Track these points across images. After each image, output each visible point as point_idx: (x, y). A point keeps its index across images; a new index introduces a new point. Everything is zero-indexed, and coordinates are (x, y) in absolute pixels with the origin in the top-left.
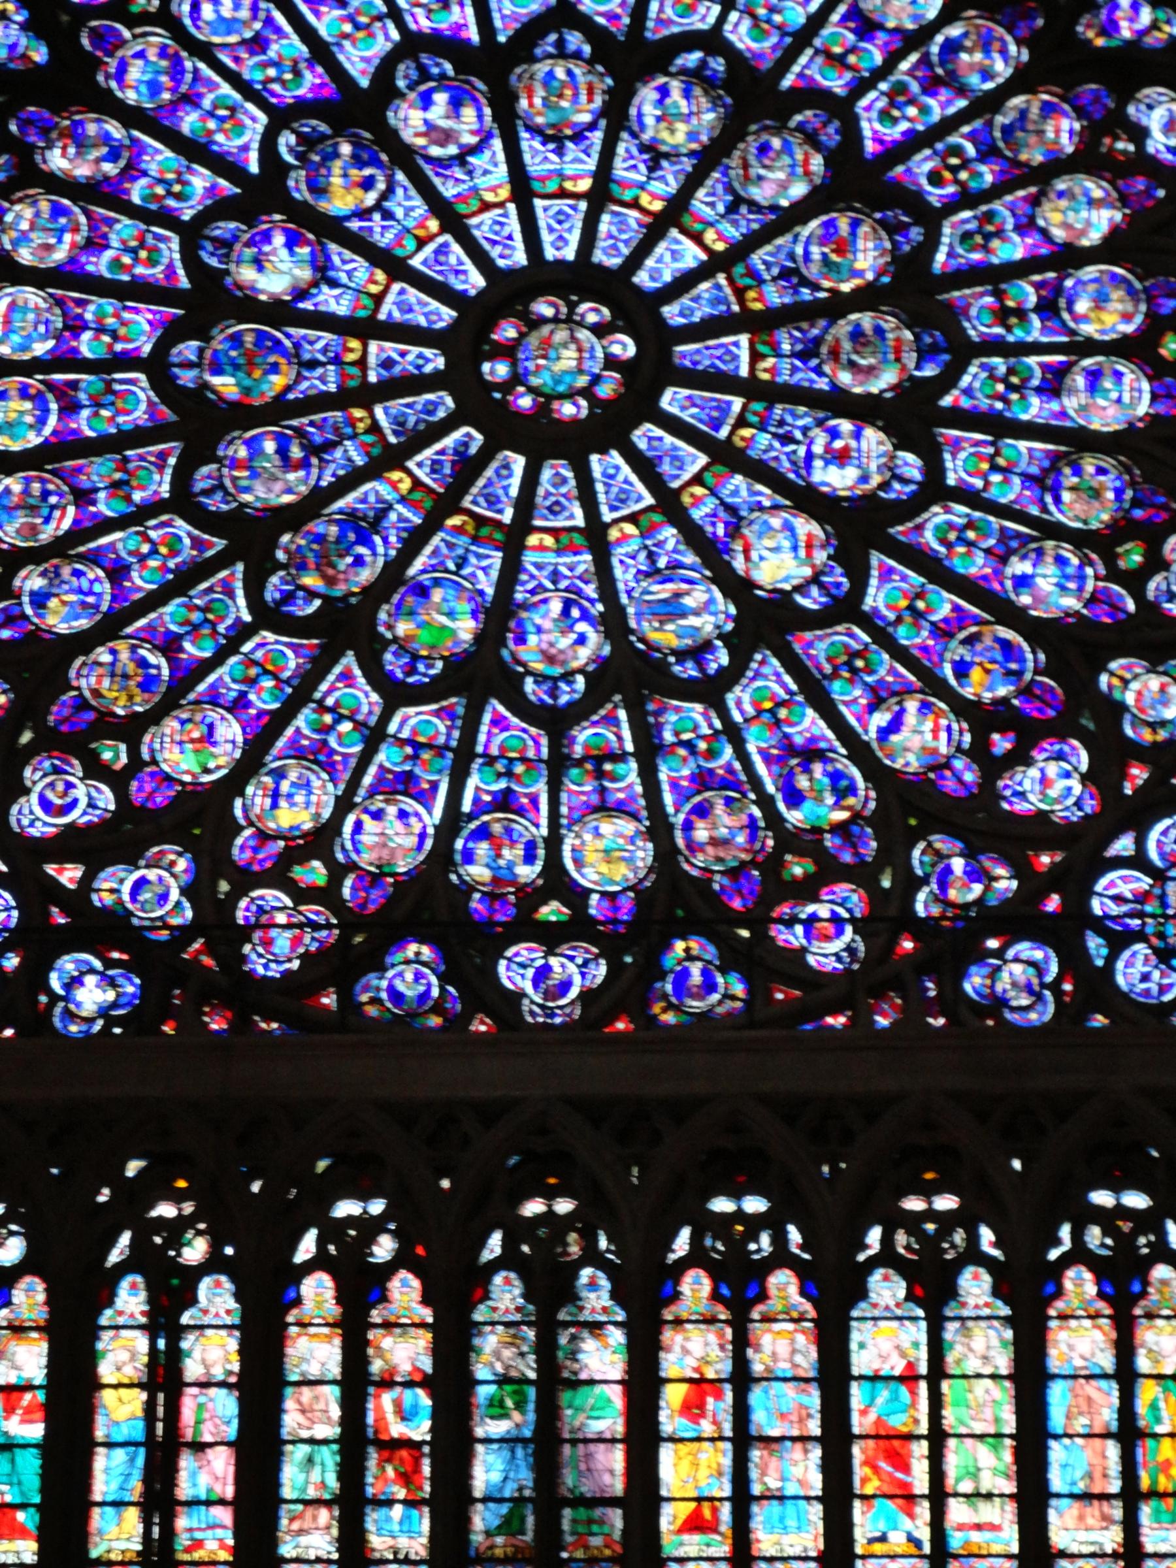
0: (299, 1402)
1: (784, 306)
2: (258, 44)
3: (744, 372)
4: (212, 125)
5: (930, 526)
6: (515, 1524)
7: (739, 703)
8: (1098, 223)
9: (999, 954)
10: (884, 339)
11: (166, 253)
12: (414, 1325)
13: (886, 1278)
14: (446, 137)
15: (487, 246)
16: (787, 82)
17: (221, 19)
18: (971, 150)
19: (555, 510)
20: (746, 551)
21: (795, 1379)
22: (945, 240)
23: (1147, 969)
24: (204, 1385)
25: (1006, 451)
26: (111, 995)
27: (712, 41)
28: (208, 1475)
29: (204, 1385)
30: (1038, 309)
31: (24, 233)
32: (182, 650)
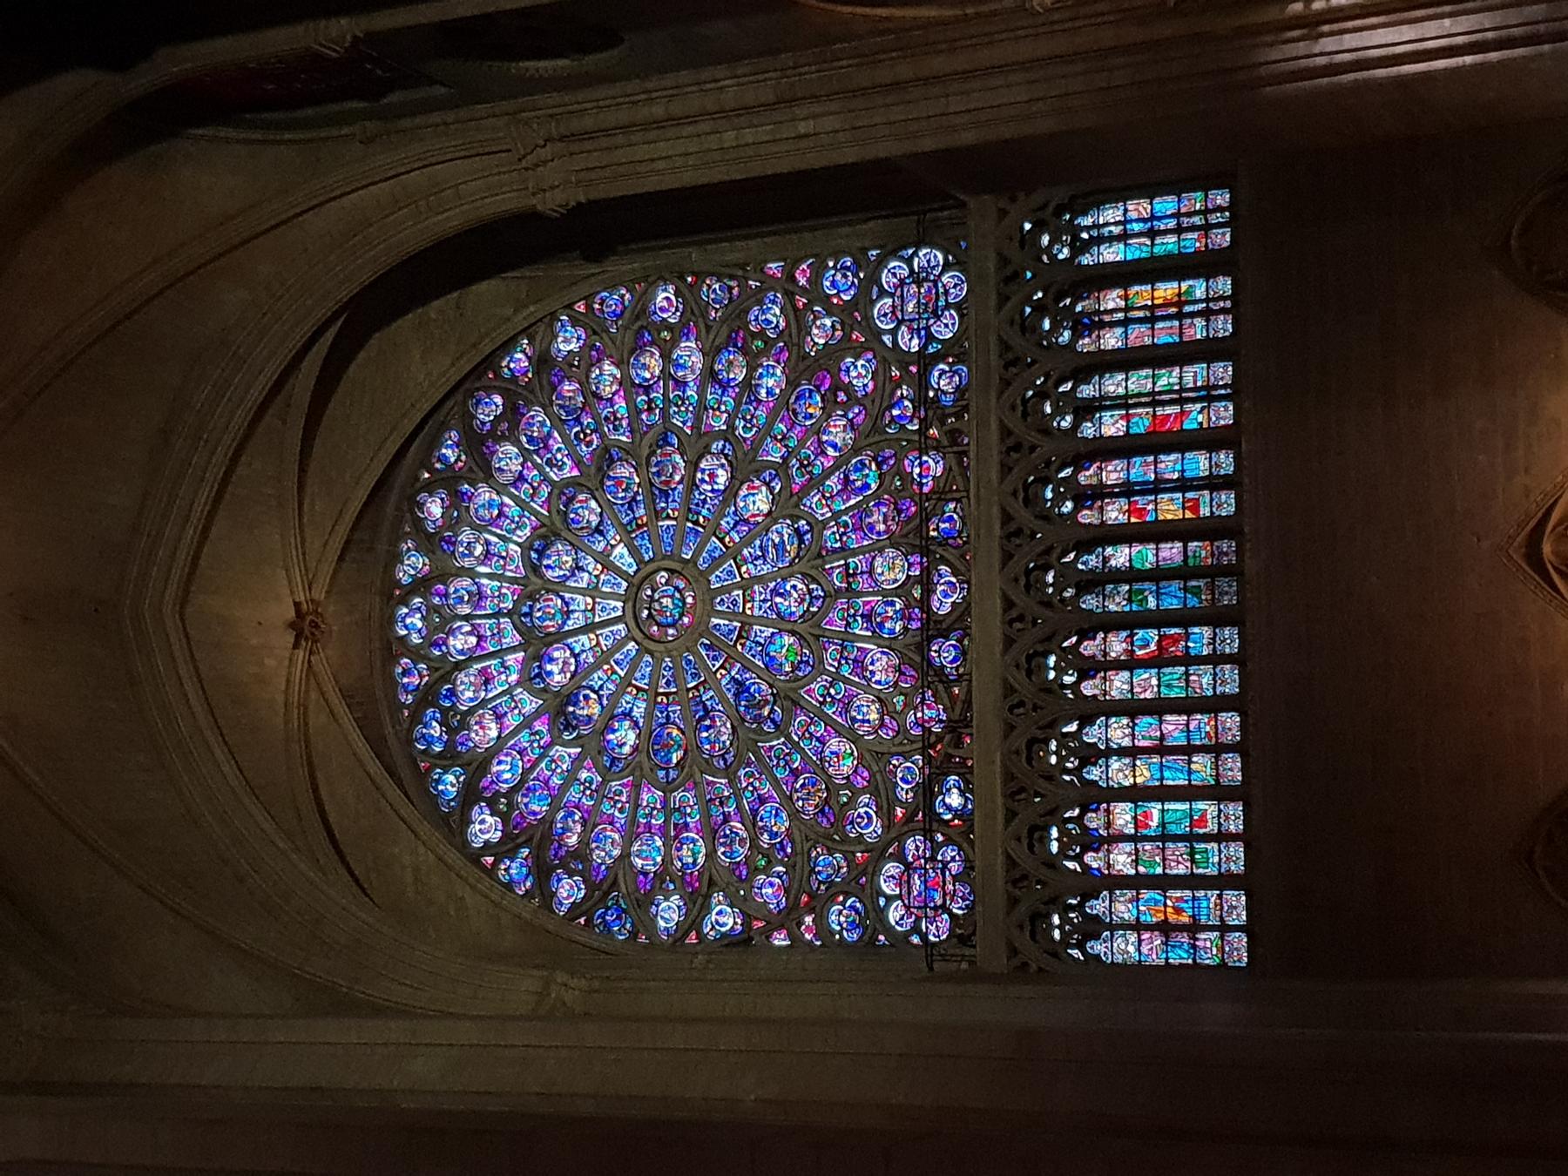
9: (936, 391)
14: (565, 663)
20: (754, 516)
28: (1173, 726)
29: (1133, 735)
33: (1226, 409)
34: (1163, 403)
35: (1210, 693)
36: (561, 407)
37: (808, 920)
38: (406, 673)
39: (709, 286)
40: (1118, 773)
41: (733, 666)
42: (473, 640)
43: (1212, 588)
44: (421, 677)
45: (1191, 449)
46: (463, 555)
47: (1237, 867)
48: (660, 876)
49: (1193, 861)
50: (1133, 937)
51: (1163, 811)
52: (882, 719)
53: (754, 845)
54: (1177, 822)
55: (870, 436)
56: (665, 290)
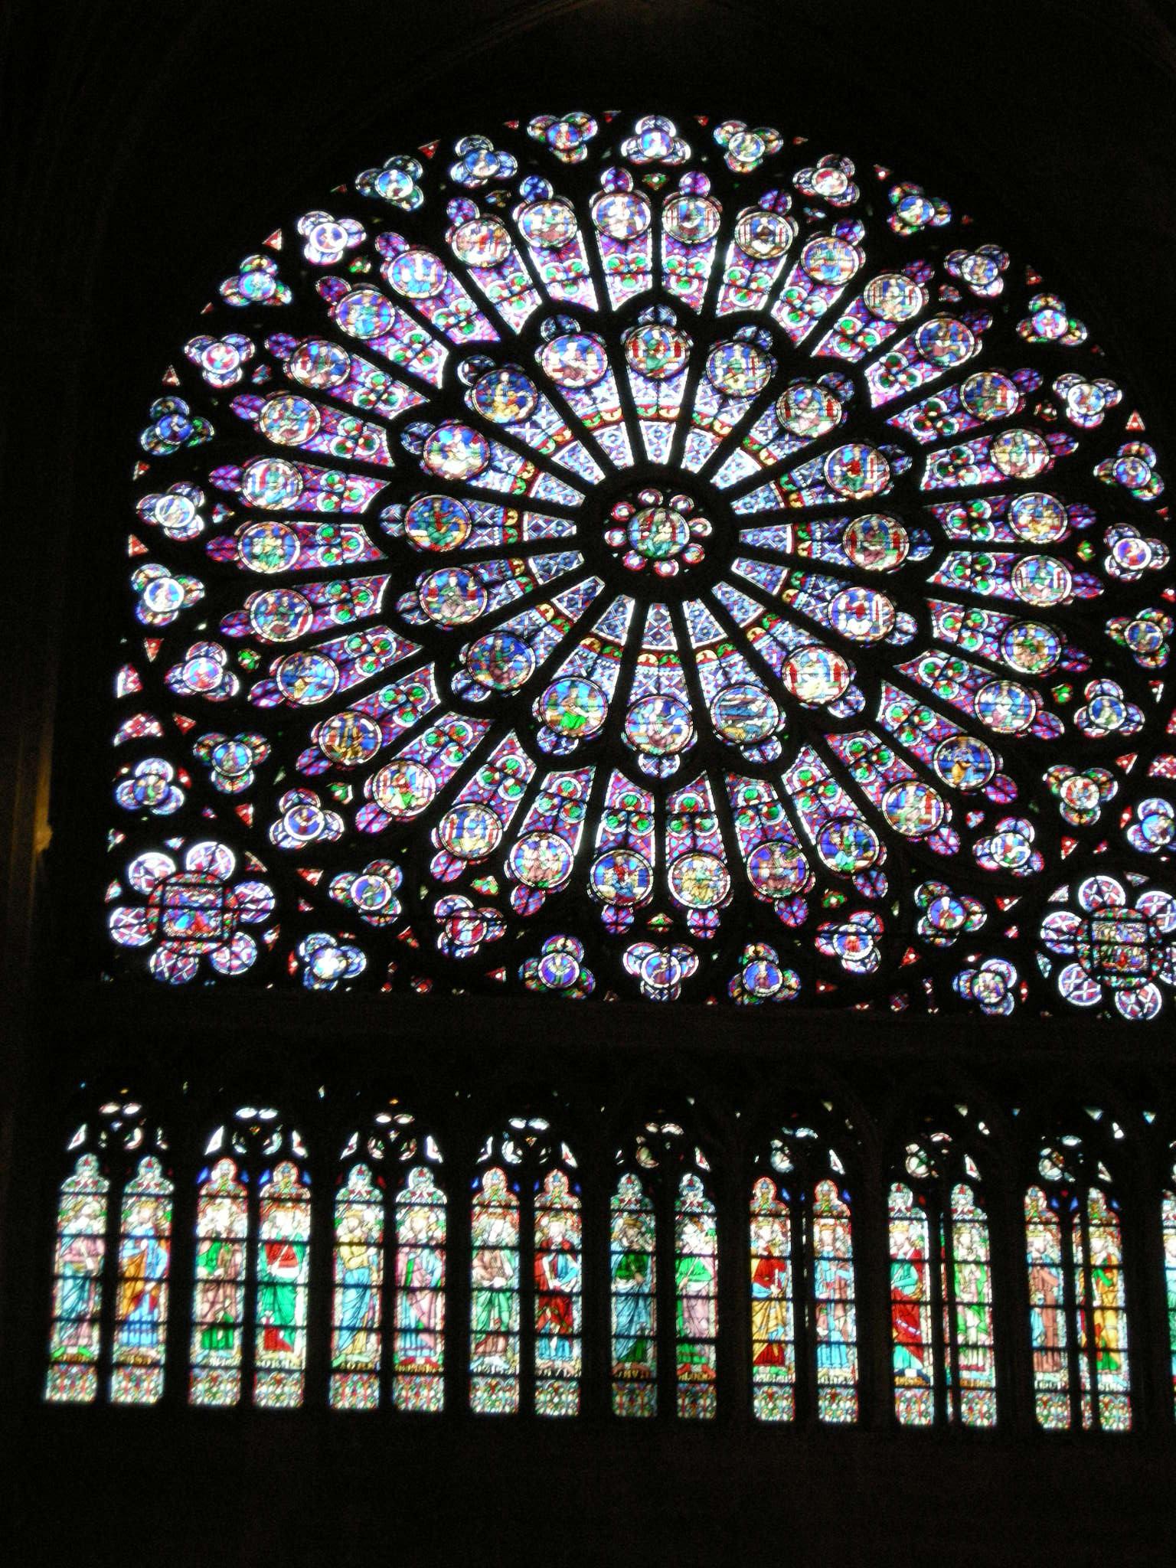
0: (482, 1260)
1: (815, 508)
2: (440, 299)
3: (789, 551)
4: (410, 354)
5: (922, 665)
6: (639, 1354)
7: (790, 781)
8: (1034, 464)
10: (886, 533)
11: (378, 441)
12: (563, 1209)
13: (898, 1190)
14: (577, 373)
15: (607, 451)
16: (814, 353)
17: (417, 282)
18: (944, 408)
19: (657, 637)
20: (793, 674)
21: (835, 1259)
22: (928, 468)
23: (1079, 981)
24: (414, 1246)
25: (973, 616)
26: (343, 964)
27: (762, 320)
29: (414, 1246)
30: (993, 519)
31: (275, 421)
32: (392, 722)
33: (921, 1414)
34: (937, 1320)
35: (474, 1366)
36: (980, 385)
37: (154, 728)
38: (576, 129)
39: (1158, 623)
40: (358, 1218)
41: (559, 628)
42: (621, 232)
43: (641, 1379)
44: (568, 151)
45: (861, 1357)
46: (753, 226)
47: (200, 1394)
48: (232, 500)
49: (213, 1326)
50: (99, 1226)
51: (294, 1285)
52: (462, 858)
53: (269, 651)
54: (275, 1306)
55: (909, 861)
56: (1155, 554)
